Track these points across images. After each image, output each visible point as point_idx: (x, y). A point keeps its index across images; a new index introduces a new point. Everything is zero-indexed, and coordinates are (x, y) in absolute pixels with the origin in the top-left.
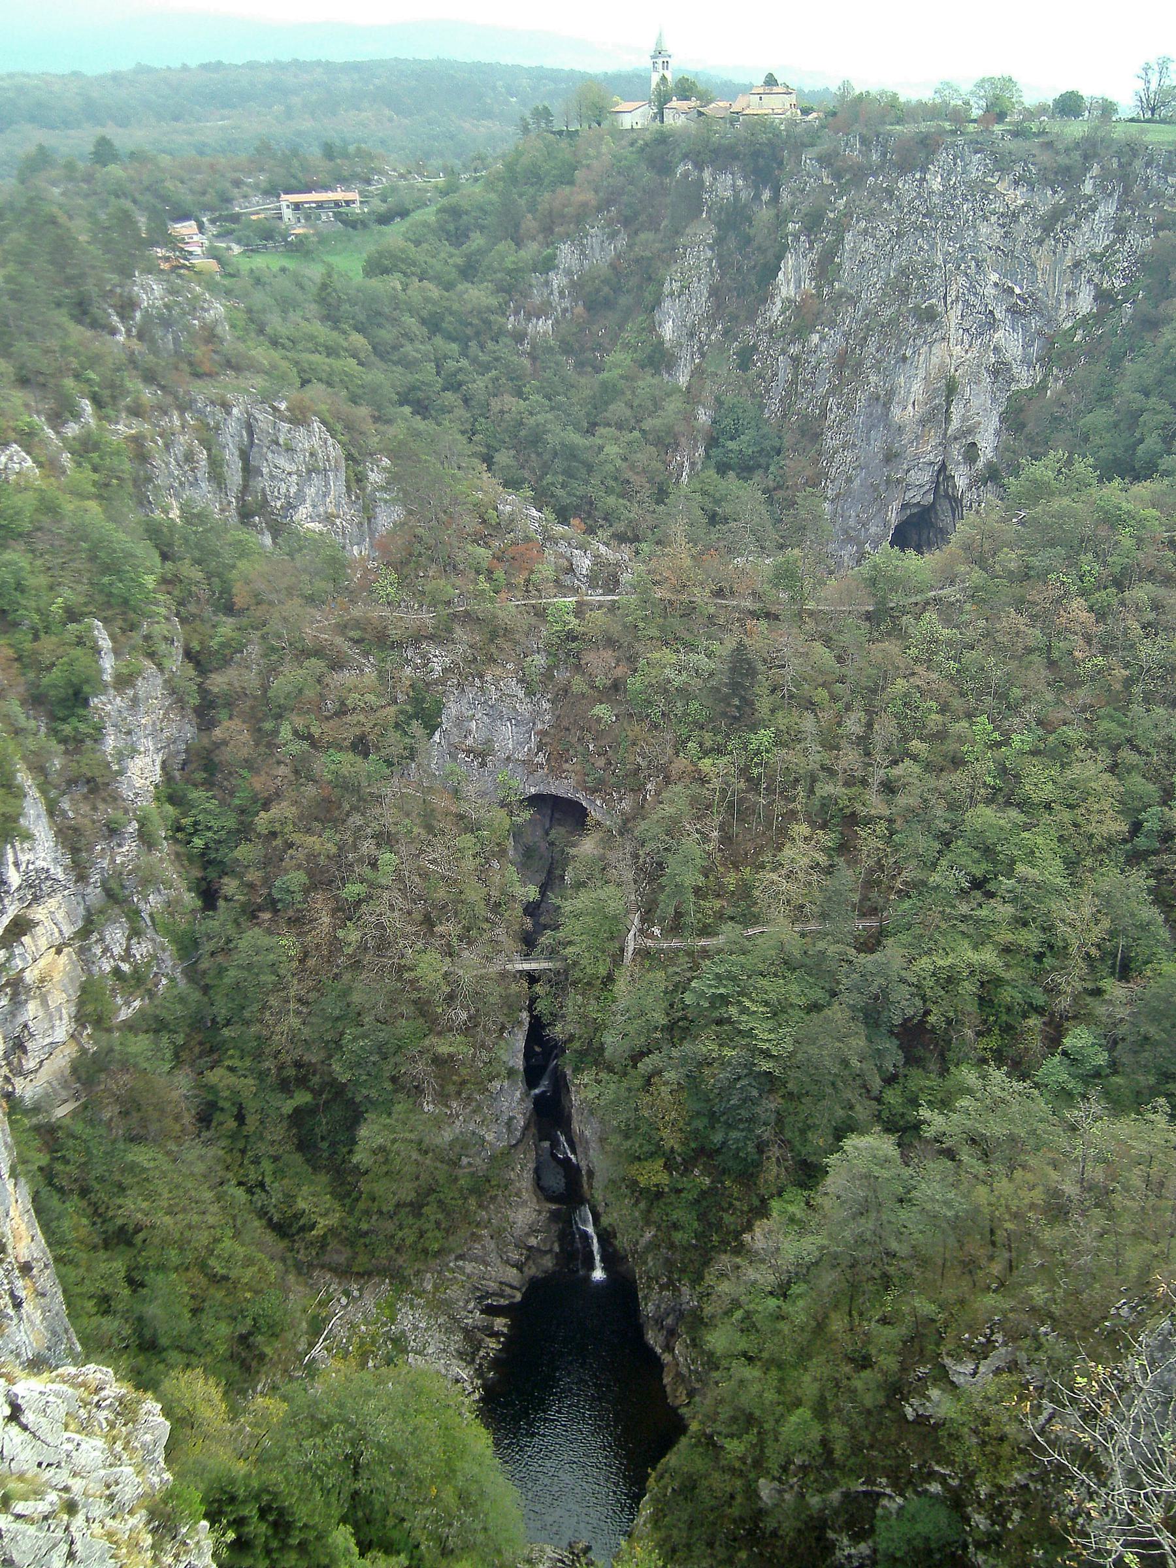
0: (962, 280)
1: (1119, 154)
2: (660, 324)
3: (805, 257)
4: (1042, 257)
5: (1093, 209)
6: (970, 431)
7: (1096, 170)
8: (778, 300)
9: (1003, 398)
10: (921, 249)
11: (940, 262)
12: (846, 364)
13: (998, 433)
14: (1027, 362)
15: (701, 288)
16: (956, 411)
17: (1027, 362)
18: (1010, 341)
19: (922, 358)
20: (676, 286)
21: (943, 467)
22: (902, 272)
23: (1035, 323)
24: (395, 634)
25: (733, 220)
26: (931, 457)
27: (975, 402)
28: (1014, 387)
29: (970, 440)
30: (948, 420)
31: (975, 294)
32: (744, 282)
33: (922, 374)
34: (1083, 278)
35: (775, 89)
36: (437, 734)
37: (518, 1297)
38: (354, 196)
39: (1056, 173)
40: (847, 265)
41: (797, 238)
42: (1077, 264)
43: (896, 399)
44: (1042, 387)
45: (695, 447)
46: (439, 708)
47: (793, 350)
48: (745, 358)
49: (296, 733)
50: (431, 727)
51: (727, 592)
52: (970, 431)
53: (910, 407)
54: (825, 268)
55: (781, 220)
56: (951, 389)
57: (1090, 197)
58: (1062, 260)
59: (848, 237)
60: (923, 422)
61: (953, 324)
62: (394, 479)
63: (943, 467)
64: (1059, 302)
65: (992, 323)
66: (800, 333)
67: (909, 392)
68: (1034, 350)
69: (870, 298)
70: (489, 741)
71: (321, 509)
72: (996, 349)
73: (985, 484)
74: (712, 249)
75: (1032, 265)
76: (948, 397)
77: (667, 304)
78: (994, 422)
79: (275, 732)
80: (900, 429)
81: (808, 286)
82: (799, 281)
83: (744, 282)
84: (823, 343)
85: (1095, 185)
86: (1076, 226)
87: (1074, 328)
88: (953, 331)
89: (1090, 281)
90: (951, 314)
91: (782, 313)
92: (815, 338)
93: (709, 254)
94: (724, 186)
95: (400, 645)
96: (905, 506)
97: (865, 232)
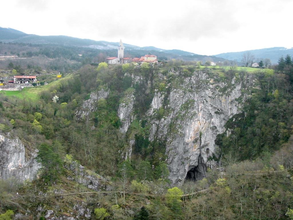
0: (202, 105)
1: (240, 74)
2: (119, 114)
3: (159, 97)
4: (223, 99)
5: (235, 88)
6: (207, 145)
7: (235, 78)
8: (152, 109)
9: (215, 136)
10: (191, 97)
11: (196, 100)
12: (172, 127)
14: (221, 126)
15: (131, 105)
16: (203, 140)
17: (221, 126)
18: (216, 121)
19: (193, 125)
20: (124, 104)
21: (200, 155)
22: (186, 102)
23: (222, 116)
25: (140, 88)
26: (197, 152)
27: (208, 137)
28: (218, 133)
29: (207, 147)
30: (201, 142)
31: (206, 109)
32: (142, 105)
33: (193, 129)
34: (234, 104)
35: (151, 56)
38: (34, 77)
39: (225, 79)
40: (171, 100)
41: (157, 92)
42: (232, 102)
43: (186, 136)
44: (225, 133)
45: (129, 149)
47: (157, 122)
48: (143, 124)
51: (139, 191)
52: (207, 145)
53: (190, 139)
54: (166, 102)
55: (152, 88)
56: (201, 134)
57: (234, 85)
58: (228, 100)
59: (171, 93)
60: (194, 142)
61: (201, 116)
62: (40, 155)
63: (200, 155)
64: (228, 111)
65: (211, 116)
66: (159, 118)
67: (190, 134)
68: (223, 123)
69: (178, 109)
71: (17, 164)
72: (213, 123)
73: (212, 160)
74: (134, 94)
75: (221, 101)
76: (200, 136)
77: (121, 109)
78: (214, 143)
80: (187, 144)
81: (160, 105)
82: (158, 104)
83: (142, 105)
84: (165, 121)
85: (235, 82)
86: (231, 92)
87: (233, 118)
88: (201, 118)
89: (236, 106)
90: (200, 114)
91: (153, 112)
92: (163, 119)
93: (133, 96)
94: (138, 79)
96: (190, 166)
97: (175, 92)
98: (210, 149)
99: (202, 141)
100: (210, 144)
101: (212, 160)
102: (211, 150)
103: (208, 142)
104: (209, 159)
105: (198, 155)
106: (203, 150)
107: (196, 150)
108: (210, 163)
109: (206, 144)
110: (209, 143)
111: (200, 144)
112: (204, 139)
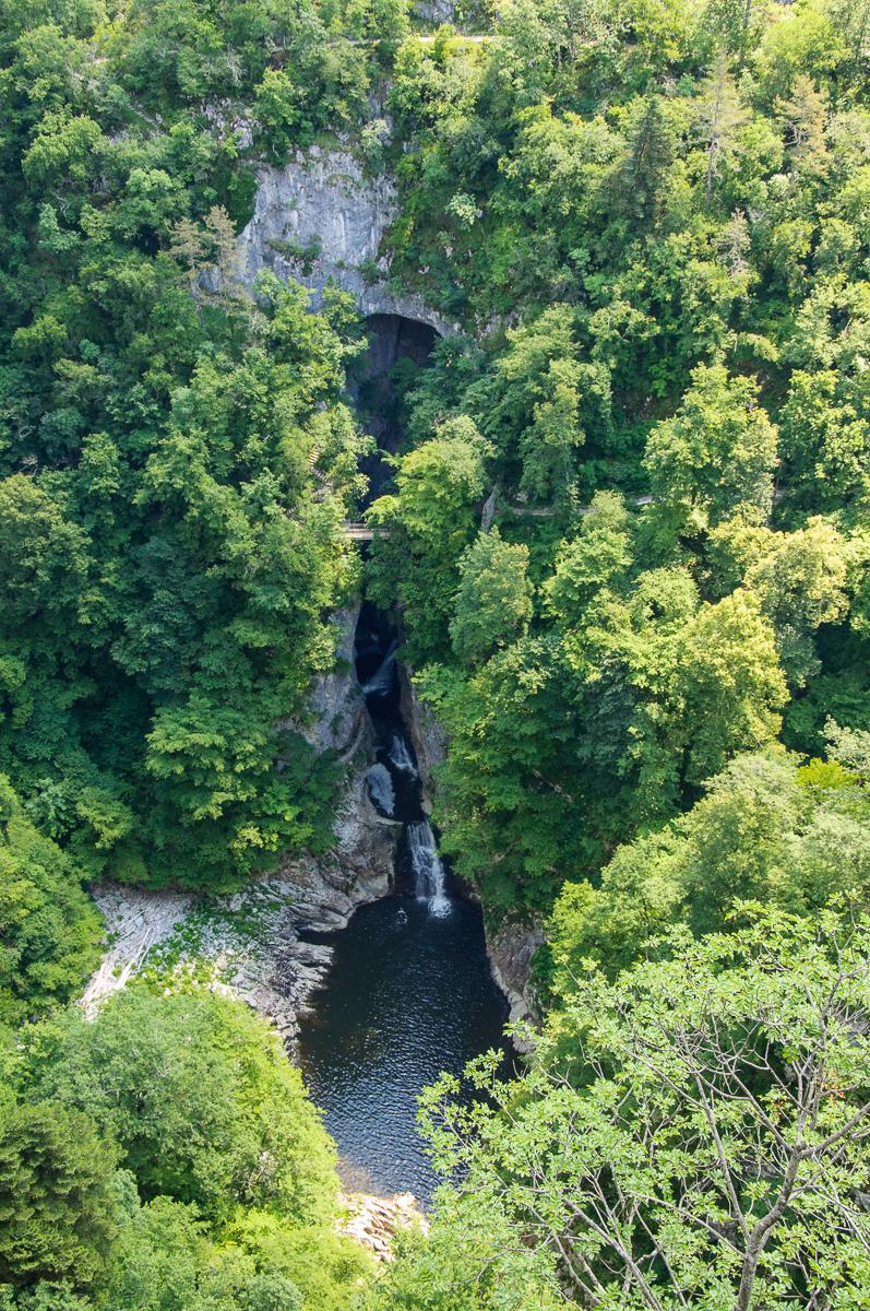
24: (191, 84)
36: (247, 229)
37: (343, 923)
46: (250, 189)
49: (62, 221)
50: (241, 217)
70: (315, 239)
79: (34, 216)
95: (195, 101)
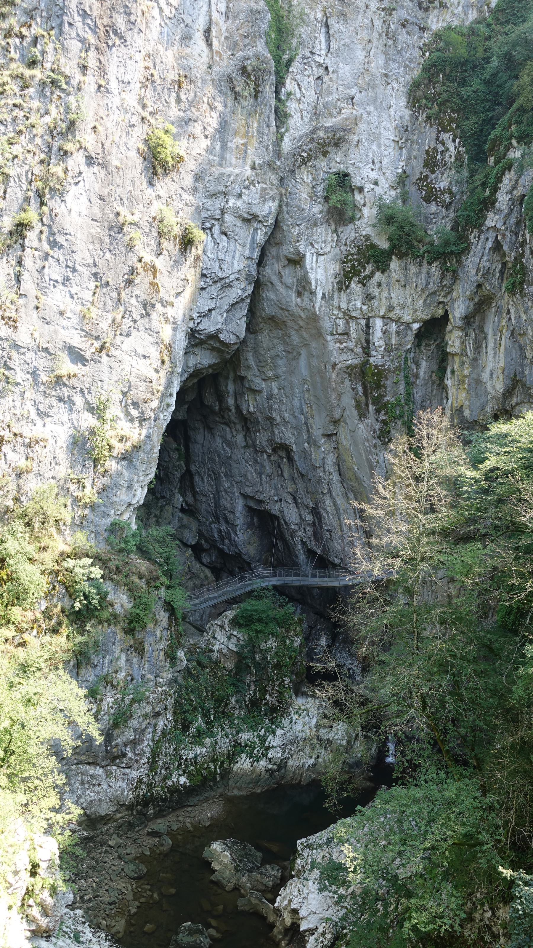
6: (336, 140)
13: (405, 134)
16: (301, 87)
26: (252, 195)
52: (336, 140)
73: (384, 269)
78: (398, 106)
98: (363, 174)
99: (292, 106)
100: (363, 126)
101: (384, 269)
102: (368, 186)
103: (347, 112)
104: (361, 264)
105: (260, 237)
106: (305, 188)
107: (248, 172)
108: (369, 298)
109: (327, 130)
110: (356, 120)
111: (279, 140)
112: (309, 84)
